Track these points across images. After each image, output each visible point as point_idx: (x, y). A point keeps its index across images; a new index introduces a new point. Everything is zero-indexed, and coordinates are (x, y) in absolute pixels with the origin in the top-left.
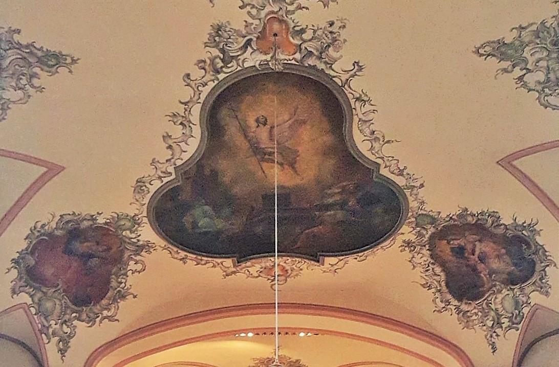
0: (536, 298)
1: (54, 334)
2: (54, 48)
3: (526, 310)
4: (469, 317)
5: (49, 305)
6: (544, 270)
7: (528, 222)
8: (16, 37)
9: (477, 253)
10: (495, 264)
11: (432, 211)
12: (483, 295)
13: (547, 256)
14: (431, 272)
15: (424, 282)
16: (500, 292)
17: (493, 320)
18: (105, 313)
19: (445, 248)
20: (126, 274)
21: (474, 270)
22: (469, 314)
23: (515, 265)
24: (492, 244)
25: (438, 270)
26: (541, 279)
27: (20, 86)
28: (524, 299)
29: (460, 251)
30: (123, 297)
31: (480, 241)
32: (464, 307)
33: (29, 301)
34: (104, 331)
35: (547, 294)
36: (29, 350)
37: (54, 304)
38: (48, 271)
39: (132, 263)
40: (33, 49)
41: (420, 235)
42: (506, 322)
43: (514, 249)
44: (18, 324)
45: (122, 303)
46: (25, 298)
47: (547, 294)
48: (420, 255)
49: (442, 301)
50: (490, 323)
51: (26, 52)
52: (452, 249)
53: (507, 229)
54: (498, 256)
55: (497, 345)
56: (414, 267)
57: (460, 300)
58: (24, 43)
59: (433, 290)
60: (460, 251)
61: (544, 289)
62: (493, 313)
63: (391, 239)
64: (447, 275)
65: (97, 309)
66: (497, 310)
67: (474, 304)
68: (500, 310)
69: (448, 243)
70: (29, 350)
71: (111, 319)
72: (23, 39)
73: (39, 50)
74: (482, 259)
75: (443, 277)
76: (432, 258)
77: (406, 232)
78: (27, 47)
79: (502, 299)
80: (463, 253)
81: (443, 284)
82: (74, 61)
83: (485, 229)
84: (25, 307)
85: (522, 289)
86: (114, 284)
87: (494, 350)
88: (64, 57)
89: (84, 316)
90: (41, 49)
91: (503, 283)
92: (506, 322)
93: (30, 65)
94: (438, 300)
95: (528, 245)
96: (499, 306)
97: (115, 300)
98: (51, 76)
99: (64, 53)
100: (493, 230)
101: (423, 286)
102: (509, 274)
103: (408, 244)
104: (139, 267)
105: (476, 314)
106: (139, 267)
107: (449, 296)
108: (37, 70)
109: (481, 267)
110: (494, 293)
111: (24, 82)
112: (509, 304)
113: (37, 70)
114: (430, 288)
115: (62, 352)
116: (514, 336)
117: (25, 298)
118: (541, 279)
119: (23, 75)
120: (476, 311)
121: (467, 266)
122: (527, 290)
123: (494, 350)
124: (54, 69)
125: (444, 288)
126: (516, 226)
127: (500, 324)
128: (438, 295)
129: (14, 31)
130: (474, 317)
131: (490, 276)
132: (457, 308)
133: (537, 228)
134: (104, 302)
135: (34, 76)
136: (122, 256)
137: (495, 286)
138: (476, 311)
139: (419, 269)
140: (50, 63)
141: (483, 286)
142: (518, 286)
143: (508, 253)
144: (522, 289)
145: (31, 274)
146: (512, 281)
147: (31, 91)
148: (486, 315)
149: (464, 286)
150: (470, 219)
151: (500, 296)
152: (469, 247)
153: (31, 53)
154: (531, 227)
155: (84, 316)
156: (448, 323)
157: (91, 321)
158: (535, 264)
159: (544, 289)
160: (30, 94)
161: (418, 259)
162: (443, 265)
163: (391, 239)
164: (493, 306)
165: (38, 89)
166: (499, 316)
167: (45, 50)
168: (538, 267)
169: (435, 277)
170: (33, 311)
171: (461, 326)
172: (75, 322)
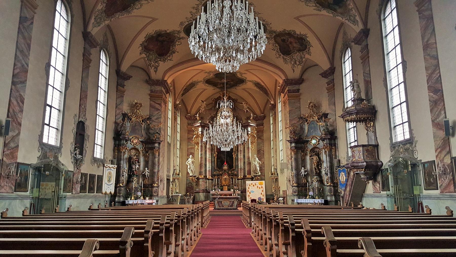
0: (307, 56)
1: (153, 66)
3: (304, 59)
5: (151, 57)
10: (295, 45)
16: (296, 53)
18: (169, 58)
19: (279, 39)
20: (175, 46)
21: (288, 45)
25: (277, 45)
29: (283, 41)
30: (174, 53)
33: (145, 56)
34: (169, 64)
36: (146, 71)
37: (153, 57)
38: (151, 47)
39: (177, 42)
42: (298, 63)
44: (141, 64)
45: (174, 55)
46: (144, 55)
52: (282, 40)
54: (296, 43)
55: (295, 70)
57: (284, 55)
61: (309, 53)
64: (280, 47)
65: (166, 57)
70: (146, 71)
71: (170, 60)
75: (279, 47)
79: (297, 56)
84: (144, 58)
86: (171, 49)
87: (294, 71)
89: (162, 60)
92: (298, 63)
97: (171, 54)
104: (180, 43)
106: (180, 43)
107: (280, 53)
109: (290, 45)
112: (299, 58)
115: (156, 71)
116: (300, 67)
117: (144, 55)
123: (294, 71)
125: (279, 51)
127: (296, 63)
132: (283, 57)
134: (168, 55)
136: (174, 40)
139: (271, 45)
145: (146, 48)
146: (299, 50)
148: (292, 60)
151: (296, 55)
155: (162, 60)
156: (280, 62)
157: (164, 61)
159: (309, 53)
161: (271, 42)
162: (278, 44)
166: (296, 61)
168: (308, 47)
170: (146, 59)
172: (159, 62)
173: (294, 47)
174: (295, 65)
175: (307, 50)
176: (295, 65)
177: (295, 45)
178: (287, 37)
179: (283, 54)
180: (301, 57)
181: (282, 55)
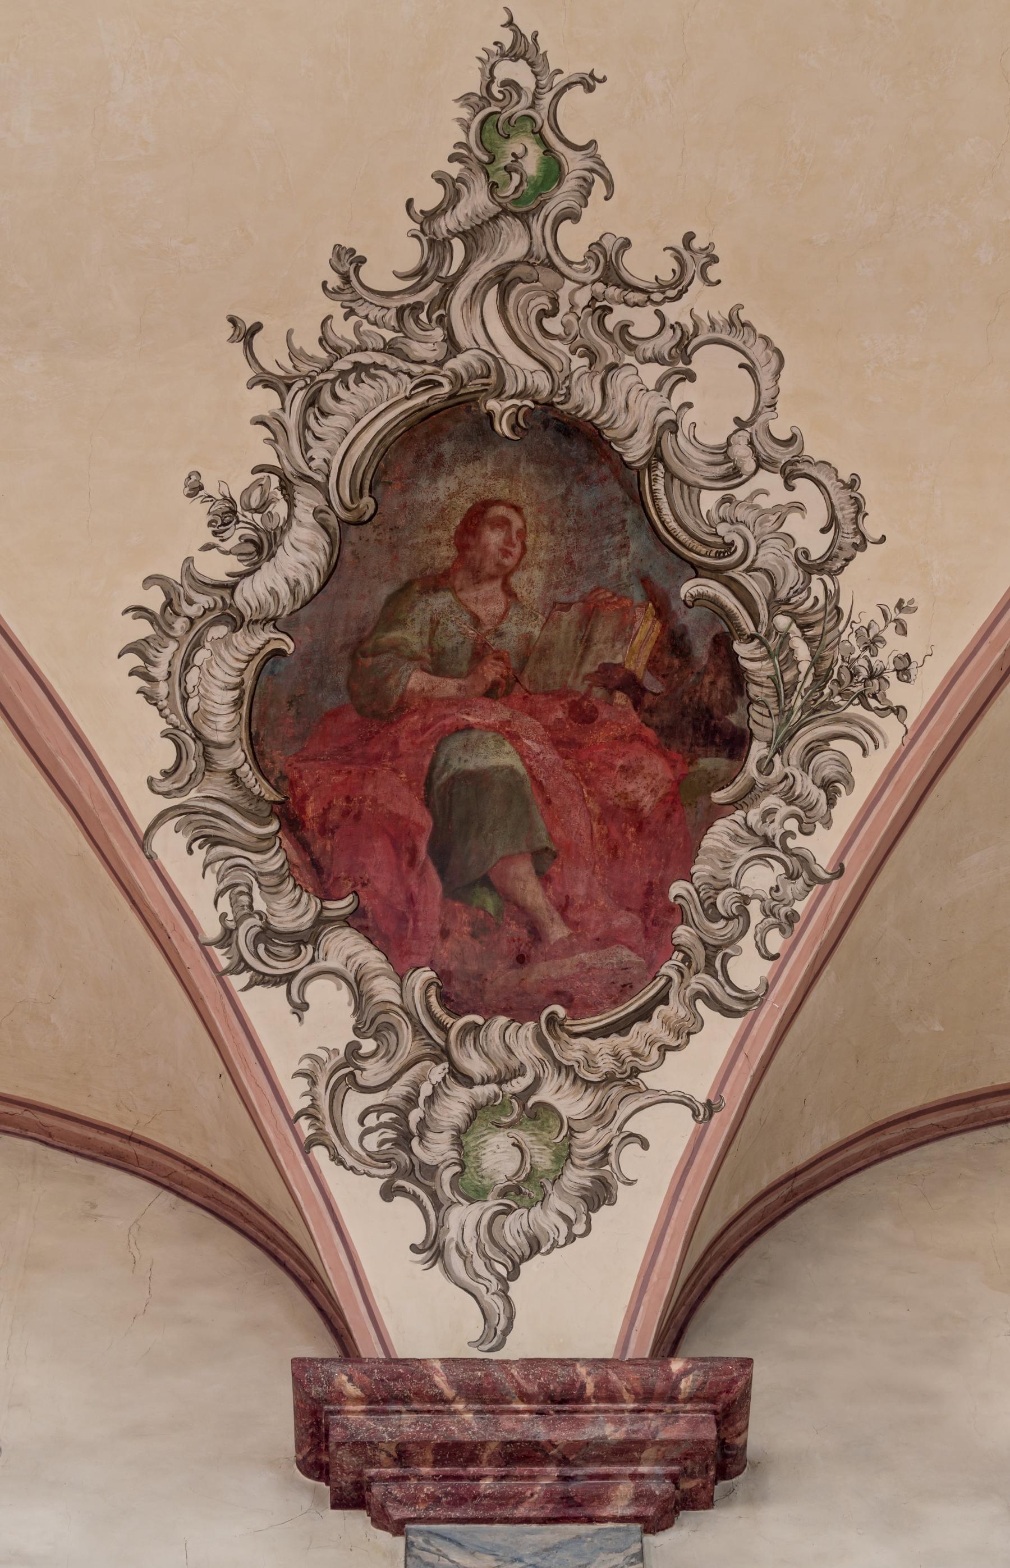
2: (442, 132)
8: (378, 275)
27: (666, 342)
40: (446, 223)
51: (467, 263)
58: (411, 255)
72: (393, 256)
73: (453, 199)
78: (438, 246)
82: (522, 48)
88: (495, 89)
90: (453, 191)
93: (543, 263)
98: (610, 185)
99: (474, 84)
108: (574, 241)
111: (643, 322)
113: (574, 241)
119: (600, 311)
124: (574, 163)
129: (346, 279)
135: (608, 264)
140: (532, 165)
147: (701, 304)
153: (473, 237)
160: (721, 314)
165: (692, 268)
167: (455, 170)
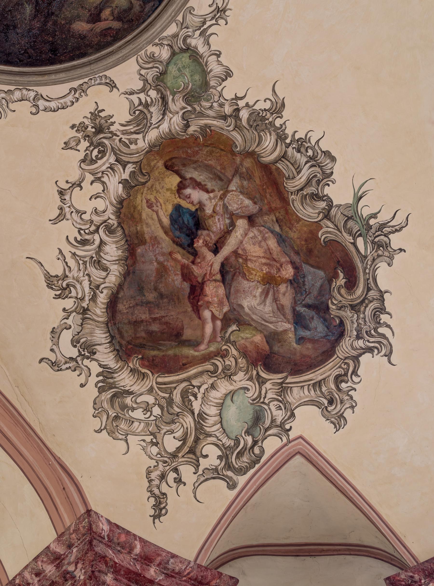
0: (309, 423)
3: (271, 444)
4: (124, 407)
6: (356, 359)
7: (382, 218)
9: (225, 251)
10: (252, 300)
11: (218, 56)
12: (184, 367)
13: (379, 323)
14: (88, 252)
15: (57, 269)
16: (228, 374)
17: (184, 440)
21: (196, 291)
22: (128, 401)
23: (299, 321)
24: (272, 243)
25: (113, 251)
26: (338, 380)
28: (279, 415)
29: (188, 226)
31: (251, 220)
32: (124, 379)
35: (339, 422)
41: (140, 119)
42: (211, 455)
43: (314, 277)
47: (339, 422)
48: (98, 187)
49: (74, 342)
50: (171, 444)
53: (327, 216)
54: (270, 282)
56: (61, 216)
59: (69, 303)
60: (188, 226)
61: (334, 406)
62: (189, 421)
63: (75, 84)
64: (126, 275)
66: (202, 416)
67: (152, 380)
68: (211, 421)
69: (181, 187)
74: (228, 273)
75: (113, 279)
76: (118, 213)
77: (116, 88)
79: (225, 397)
80: (192, 236)
81: (103, 298)
83: (282, 196)
85: (283, 389)
91: (244, 353)
92: (211, 455)
94: (66, 336)
95: (351, 284)
96: (212, 411)
100: (298, 204)
101: (50, 281)
102: (273, 337)
103: (97, 129)
105: (147, 409)
107: (100, 336)
109: (214, 291)
110: (213, 373)
112: (236, 416)
114: (64, 292)
118: (338, 380)
120: (150, 399)
121: (187, 275)
122: (296, 395)
125: (99, 311)
126: (351, 214)
127: (194, 453)
128: (74, 320)
130: (138, 414)
131: (224, 328)
132: (107, 373)
133: (396, 240)
137: (224, 355)
138: (150, 399)
139: (69, 229)
141: (194, 344)
142: (277, 378)
143: (296, 282)
144: (283, 389)
146: (267, 360)
149: (150, 322)
150: (269, 141)
151: (224, 387)
152: (218, 224)
154: (380, 236)
158: (341, 335)
159: (334, 406)
163: (75, 84)
164: (196, 406)
166: (201, 432)
168: (345, 347)
169: (92, 270)
171: (97, 423)
173: (234, 318)
174: (187, 472)
175: (328, 371)
176: (187, 472)
177: (252, 300)
178: (238, 202)
179: (124, 350)
180: (257, 419)
181: (106, 356)
